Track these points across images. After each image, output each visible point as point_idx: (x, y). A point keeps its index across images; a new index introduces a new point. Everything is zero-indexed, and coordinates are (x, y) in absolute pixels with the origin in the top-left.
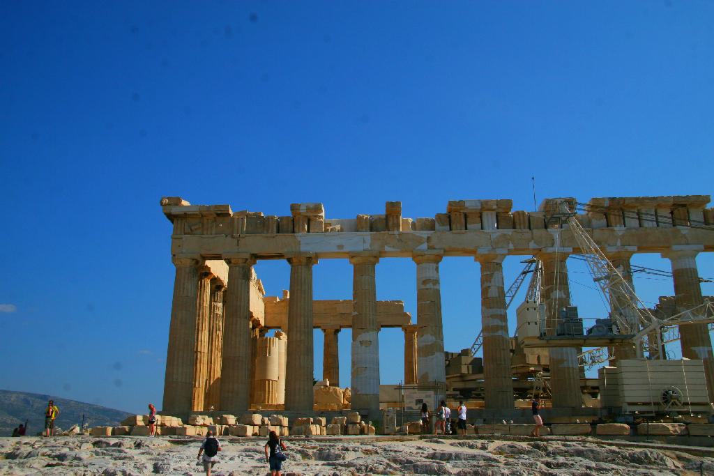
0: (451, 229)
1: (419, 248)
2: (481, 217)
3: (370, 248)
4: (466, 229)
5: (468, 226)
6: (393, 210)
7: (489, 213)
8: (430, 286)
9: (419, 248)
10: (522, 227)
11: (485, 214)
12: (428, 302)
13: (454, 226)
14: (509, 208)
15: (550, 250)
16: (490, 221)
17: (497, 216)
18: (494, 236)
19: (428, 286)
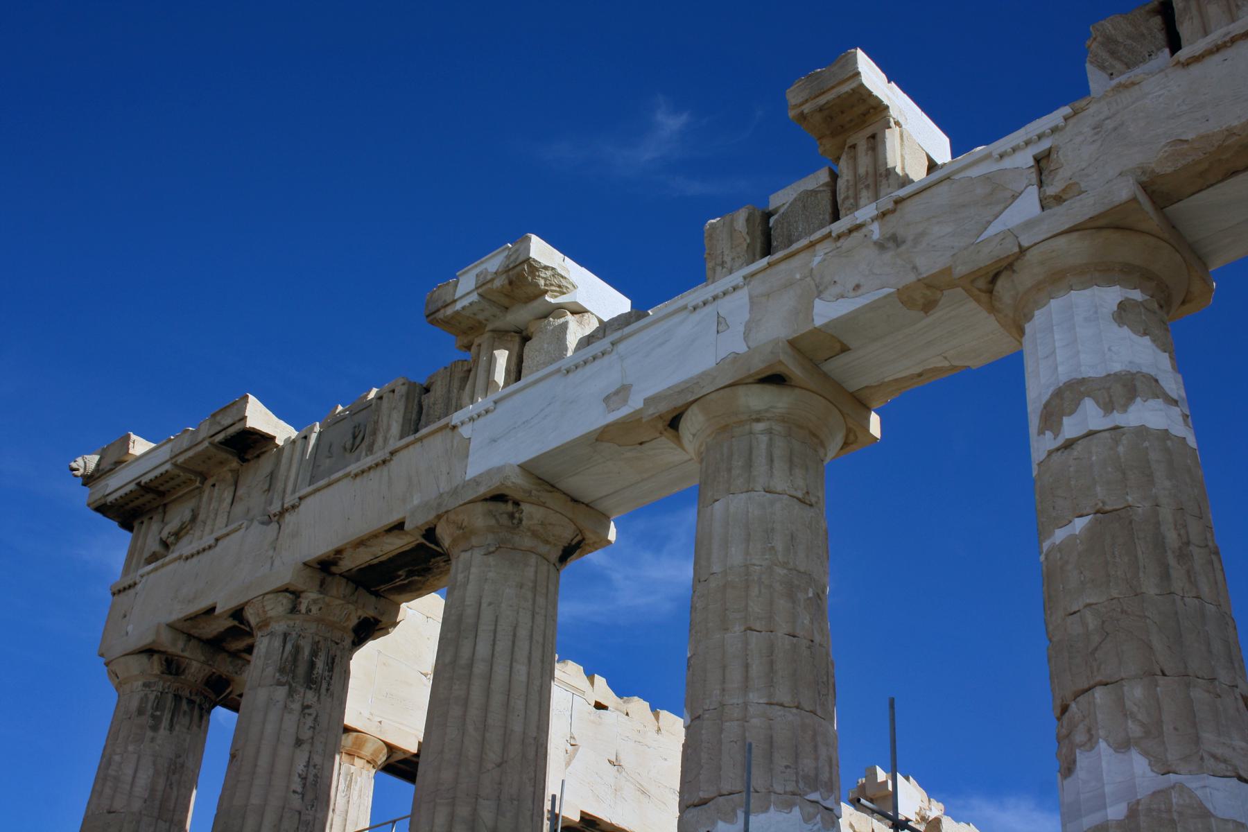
9: (991, 230)
12: (1079, 524)
19: (1071, 427)
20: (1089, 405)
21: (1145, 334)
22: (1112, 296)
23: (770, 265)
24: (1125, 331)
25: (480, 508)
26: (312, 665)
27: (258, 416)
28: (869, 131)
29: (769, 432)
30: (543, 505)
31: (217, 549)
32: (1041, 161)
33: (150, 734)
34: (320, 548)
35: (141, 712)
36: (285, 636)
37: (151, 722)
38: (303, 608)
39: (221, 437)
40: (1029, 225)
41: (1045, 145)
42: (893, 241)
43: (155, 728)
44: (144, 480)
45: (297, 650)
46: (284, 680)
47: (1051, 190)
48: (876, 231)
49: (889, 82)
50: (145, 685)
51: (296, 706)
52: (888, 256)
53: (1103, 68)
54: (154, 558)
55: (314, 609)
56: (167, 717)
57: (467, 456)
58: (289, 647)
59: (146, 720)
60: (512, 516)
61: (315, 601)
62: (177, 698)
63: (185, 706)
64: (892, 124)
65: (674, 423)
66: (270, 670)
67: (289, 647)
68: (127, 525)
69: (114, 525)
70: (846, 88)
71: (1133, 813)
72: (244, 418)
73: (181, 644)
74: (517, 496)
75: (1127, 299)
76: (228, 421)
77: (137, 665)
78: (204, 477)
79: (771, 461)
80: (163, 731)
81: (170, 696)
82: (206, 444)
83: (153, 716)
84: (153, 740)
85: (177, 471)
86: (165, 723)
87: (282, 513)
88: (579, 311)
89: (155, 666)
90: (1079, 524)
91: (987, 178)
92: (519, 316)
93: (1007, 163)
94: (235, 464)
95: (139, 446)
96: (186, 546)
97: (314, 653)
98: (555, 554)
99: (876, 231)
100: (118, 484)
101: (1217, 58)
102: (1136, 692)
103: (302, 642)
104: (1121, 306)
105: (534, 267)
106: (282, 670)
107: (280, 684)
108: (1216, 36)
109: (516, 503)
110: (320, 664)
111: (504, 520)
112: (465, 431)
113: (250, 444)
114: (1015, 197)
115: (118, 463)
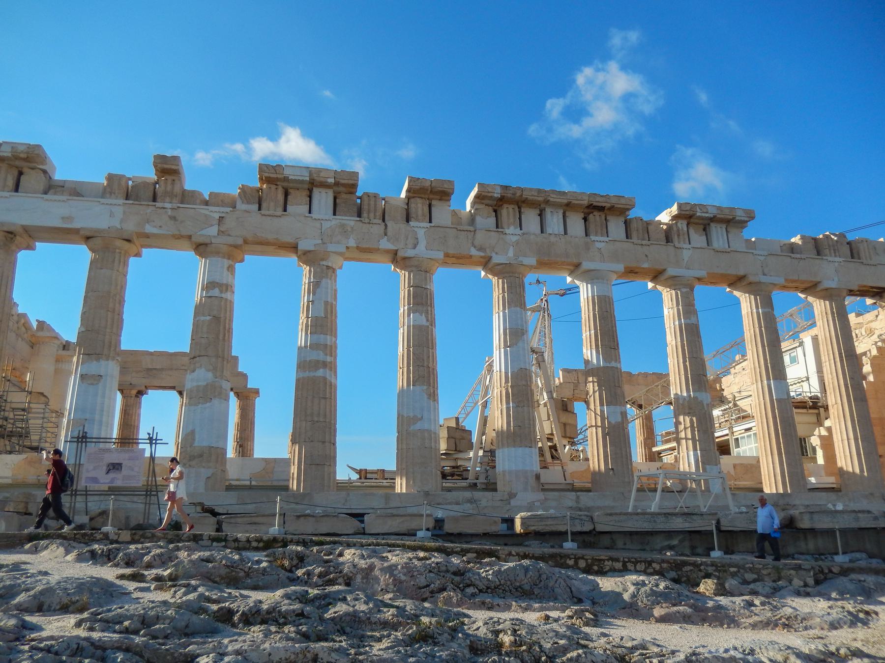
0: (260, 209)
1: (203, 232)
2: (310, 197)
3: (119, 227)
4: (285, 210)
5: (288, 207)
6: (168, 168)
7: (323, 191)
8: (216, 292)
9: (203, 232)
10: (372, 215)
11: (316, 191)
12: (208, 318)
13: (264, 205)
14: (354, 186)
15: (410, 253)
16: (323, 199)
17: (335, 198)
18: (326, 225)
28: (173, 178)
32: (221, 218)
40: (214, 237)
41: (223, 215)
42: (173, 218)
47: (222, 229)
48: (170, 212)
52: (172, 222)
71: (207, 385)
90: (208, 318)
91: (206, 215)
93: (211, 214)
99: (170, 212)
101: (269, 218)
102: (214, 360)
108: (271, 212)
114: (212, 225)
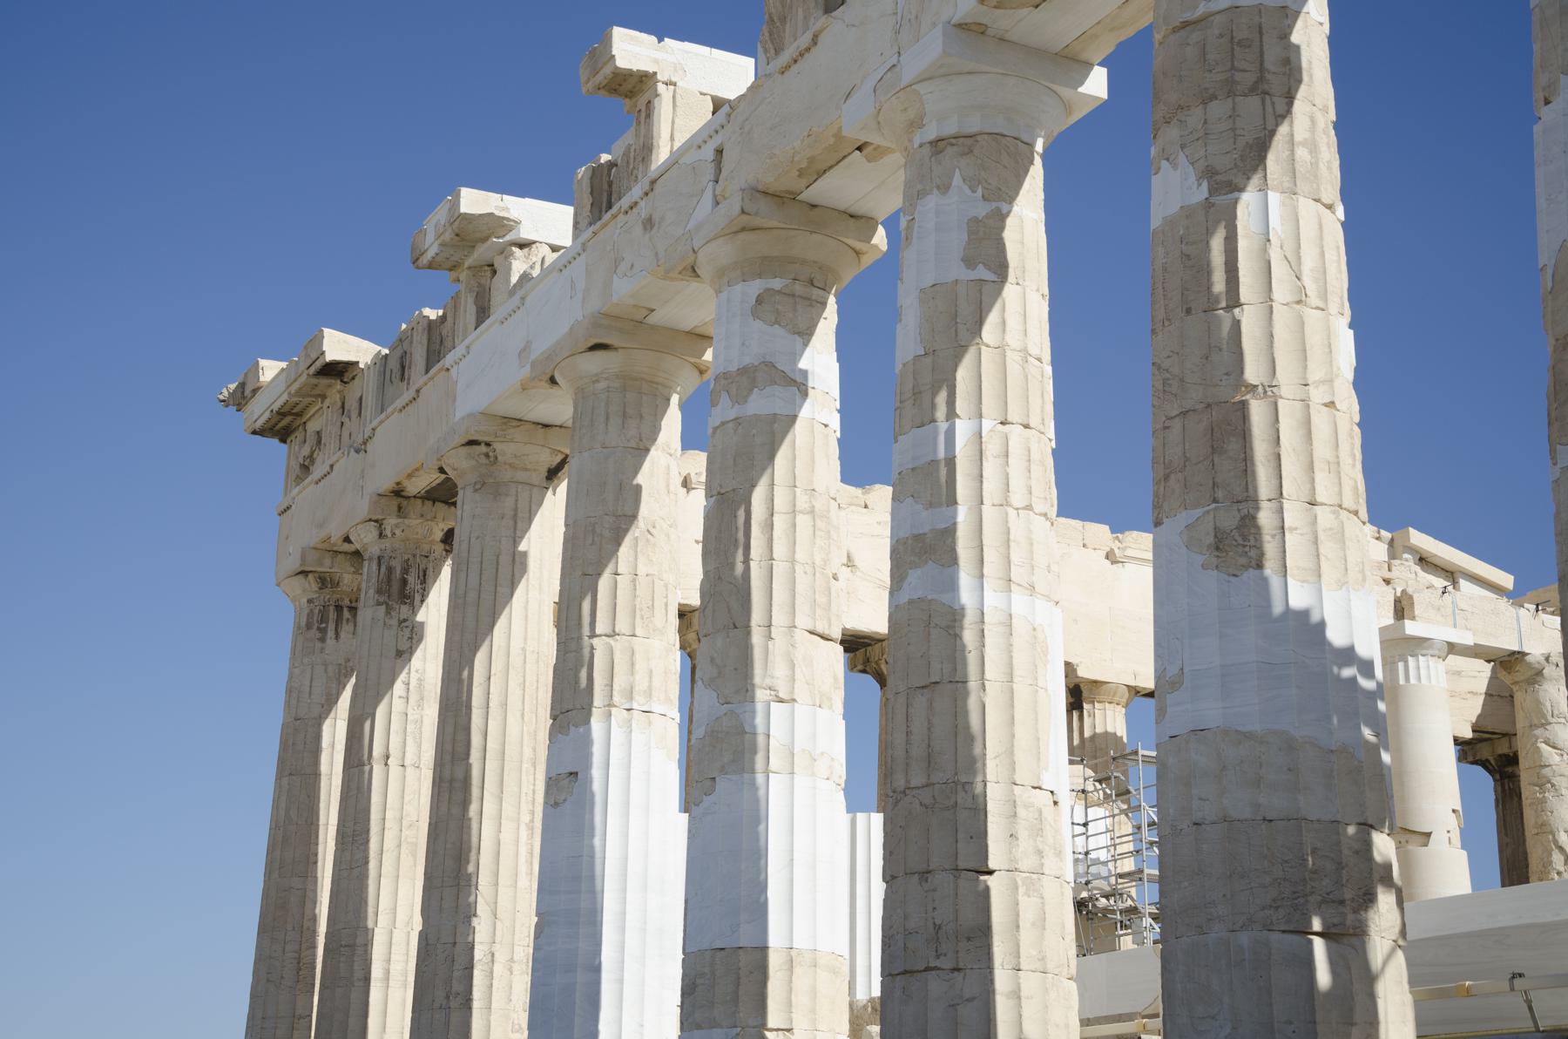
20: (725, 400)
21: (777, 322)
22: (755, 287)
23: (595, 233)
24: (758, 324)
25: (464, 451)
26: (404, 582)
27: (339, 346)
29: (608, 389)
30: (512, 441)
31: (333, 474)
32: (719, 152)
33: (319, 645)
34: (387, 484)
35: (309, 626)
36: (379, 558)
37: (319, 635)
38: (388, 532)
39: (312, 370)
43: (323, 640)
44: (276, 407)
45: (390, 570)
46: (381, 600)
49: (660, 40)
50: (310, 601)
51: (394, 622)
53: (766, 51)
54: (299, 480)
55: (398, 532)
56: (331, 626)
57: (454, 400)
58: (383, 569)
59: (314, 633)
60: (487, 456)
61: (397, 526)
62: (339, 608)
63: (346, 614)
64: (661, 88)
65: (553, 381)
66: (371, 592)
67: (383, 569)
68: (283, 441)
69: (276, 441)
70: (607, 70)
72: (323, 353)
73: (327, 562)
74: (487, 439)
75: (768, 290)
76: (314, 356)
77: (298, 584)
78: (324, 397)
79: (607, 418)
80: (330, 641)
81: (332, 609)
82: (304, 376)
83: (319, 629)
84: (322, 650)
85: (295, 399)
86: (331, 633)
87: (365, 443)
88: (524, 245)
89: (312, 584)
92: (480, 254)
94: (338, 386)
95: (270, 369)
96: (318, 470)
97: (406, 570)
98: (539, 477)
100: (259, 410)
101: (795, 68)
103: (393, 563)
104: (759, 300)
105: (469, 218)
106: (379, 591)
107: (379, 604)
109: (488, 444)
110: (412, 579)
111: (483, 460)
112: (453, 371)
113: (339, 371)
115: (255, 391)
